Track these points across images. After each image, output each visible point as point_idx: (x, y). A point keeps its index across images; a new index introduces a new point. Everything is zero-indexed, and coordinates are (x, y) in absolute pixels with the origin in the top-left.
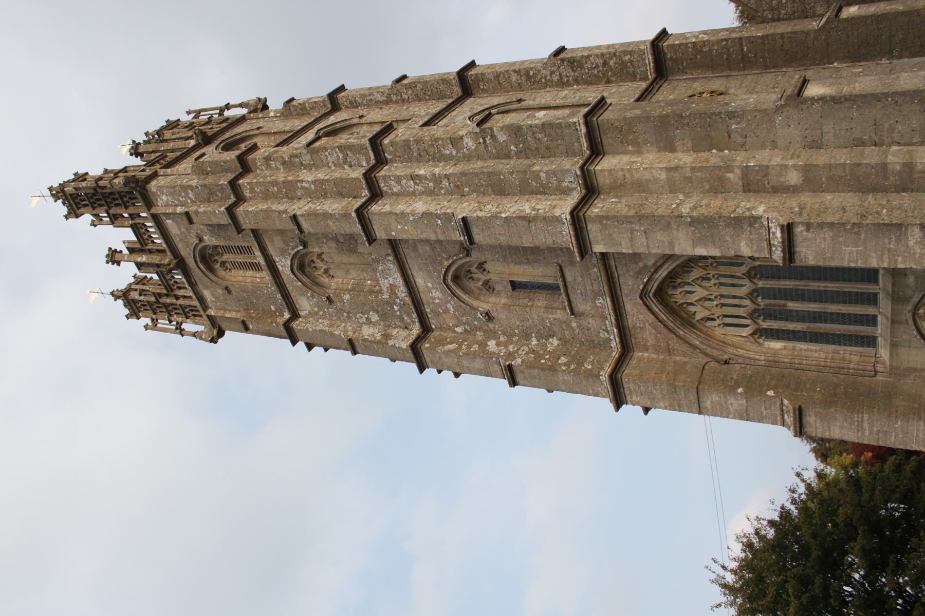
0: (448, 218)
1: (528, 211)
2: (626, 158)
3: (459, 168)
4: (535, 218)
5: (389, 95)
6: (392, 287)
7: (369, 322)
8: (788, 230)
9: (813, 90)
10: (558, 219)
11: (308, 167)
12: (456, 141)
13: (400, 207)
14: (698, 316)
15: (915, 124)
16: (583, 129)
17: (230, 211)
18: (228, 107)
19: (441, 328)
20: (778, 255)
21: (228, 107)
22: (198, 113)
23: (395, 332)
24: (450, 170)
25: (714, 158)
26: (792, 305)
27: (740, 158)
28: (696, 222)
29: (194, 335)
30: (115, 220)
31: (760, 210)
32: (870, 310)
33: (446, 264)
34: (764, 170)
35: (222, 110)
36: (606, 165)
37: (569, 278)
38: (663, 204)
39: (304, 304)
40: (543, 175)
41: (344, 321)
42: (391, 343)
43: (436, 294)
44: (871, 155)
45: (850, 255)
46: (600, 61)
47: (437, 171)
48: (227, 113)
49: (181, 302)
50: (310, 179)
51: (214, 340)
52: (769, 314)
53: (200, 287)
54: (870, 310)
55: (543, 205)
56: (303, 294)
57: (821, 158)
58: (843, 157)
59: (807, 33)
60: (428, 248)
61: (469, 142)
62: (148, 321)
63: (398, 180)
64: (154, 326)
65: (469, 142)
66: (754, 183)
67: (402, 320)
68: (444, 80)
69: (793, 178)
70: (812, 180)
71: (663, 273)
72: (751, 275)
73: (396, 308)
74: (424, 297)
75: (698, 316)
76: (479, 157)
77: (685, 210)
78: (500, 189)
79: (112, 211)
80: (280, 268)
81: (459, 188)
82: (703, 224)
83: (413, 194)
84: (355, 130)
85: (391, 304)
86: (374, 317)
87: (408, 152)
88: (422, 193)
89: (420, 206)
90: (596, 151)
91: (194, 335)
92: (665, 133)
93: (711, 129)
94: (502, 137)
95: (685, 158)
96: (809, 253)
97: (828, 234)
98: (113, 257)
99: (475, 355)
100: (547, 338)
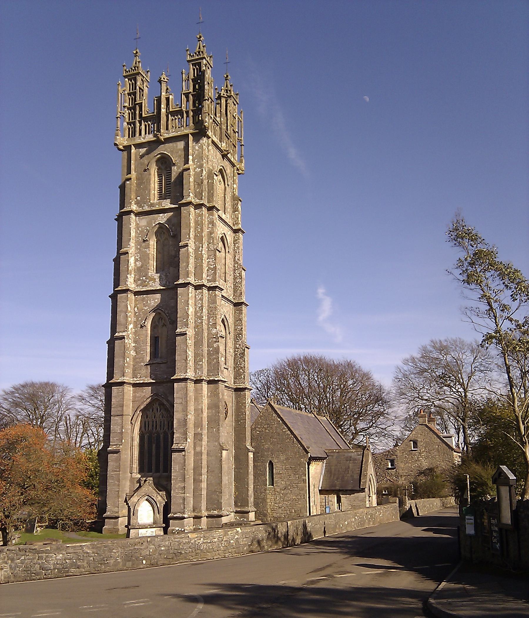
0: (187, 325)
1: (189, 359)
2: (206, 393)
3: (205, 327)
4: (187, 363)
5: (237, 263)
7: (136, 260)
8: (183, 450)
9: (224, 452)
10: (186, 372)
11: (208, 247)
12: (215, 325)
13: (190, 302)
14: (148, 413)
15: (213, 482)
16: (216, 379)
17: (190, 203)
19: (136, 300)
23: (133, 275)
24: (205, 322)
25: (205, 423)
26: (154, 446)
27: (205, 432)
28: (185, 420)
31: (189, 440)
32: (153, 470)
33: (166, 312)
34: (201, 440)
36: (205, 385)
37: (162, 365)
38: (191, 408)
39: (144, 221)
40: (201, 363)
41: (136, 245)
42: (129, 276)
44: (204, 471)
45: (175, 468)
46: (242, 366)
47: (204, 318)
49: (138, 124)
50: (203, 252)
52: (150, 438)
54: (153, 470)
55: (191, 363)
56: (149, 224)
57: (204, 457)
58: (204, 463)
59: (245, 442)
60: (172, 305)
61: (214, 331)
63: (201, 299)
65: (214, 331)
66: (198, 437)
67: (139, 280)
69: (198, 449)
70: (198, 455)
71: (165, 403)
72: (166, 434)
73: (144, 278)
75: (148, 413)
76: (208, 334)
77: (189, 417)
78: (198, 343)
79: (191, 97)
80: (161, 215)
81: (198, 327)
82: (185, 422)
83: (195, 305)
84: (223, 249)
86: (139, 264)
87: (213, 301)
88: (196, 309)
89: (191, 310)
90: (210, 382)
92: (214, 406)
93: (214, 422)
94: (215, 345)
95: (205, 414)
96: (174, 455)
97: (182, 461)
99: (127, 320)
100: (135, 350)
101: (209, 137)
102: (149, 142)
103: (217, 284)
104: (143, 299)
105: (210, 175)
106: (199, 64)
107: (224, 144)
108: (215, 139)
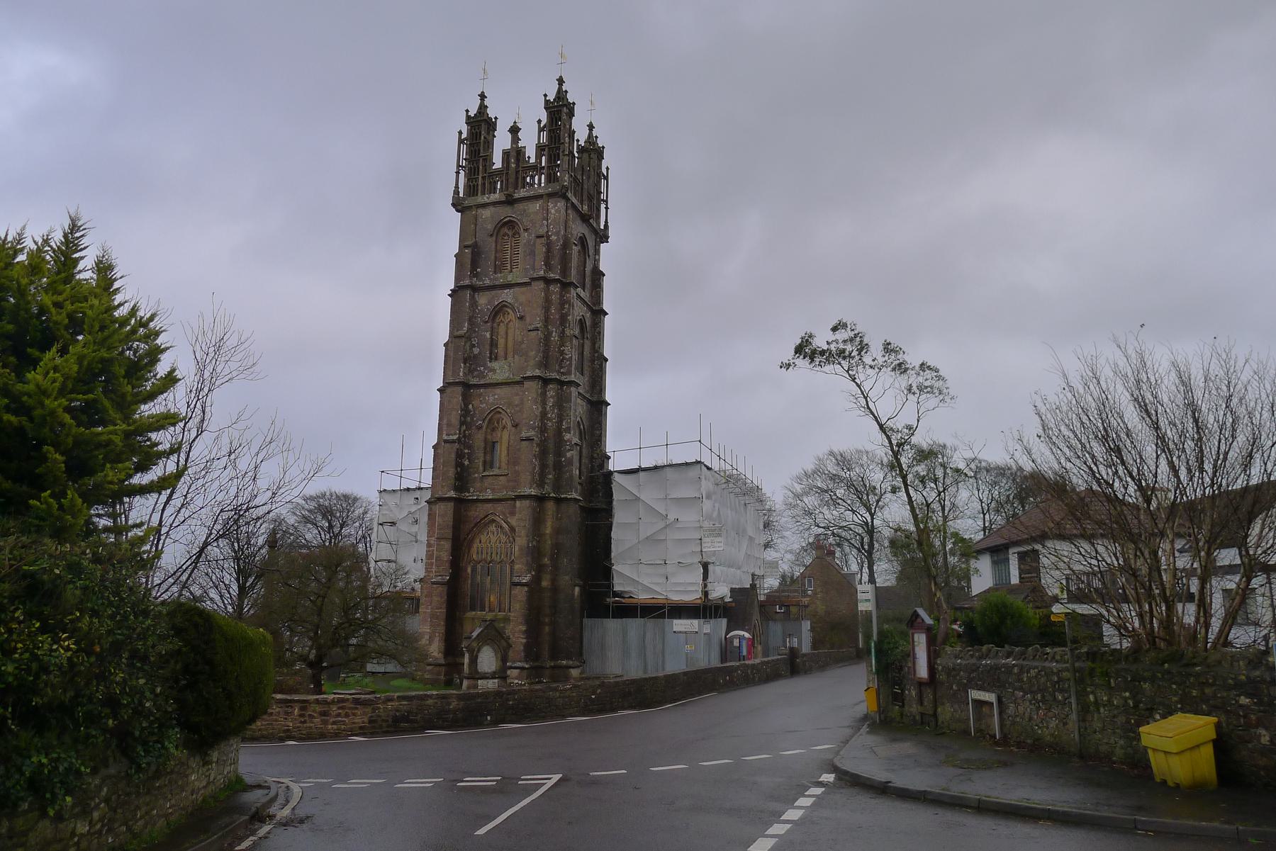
6: (494, 370)
18: (607, 208)
20: (516, 580)
21: (607, 208)
22: (606, 178)
29: (457, 187)
30: (540, 149)
35: (606, 201)
43: (491, 399)
48: (603, 206)
51: (453, 205)
53: (492, 208)
56: (489, 303)
62: (464, 136)
64: (461, 141)
68: (601, 390)
71: (505, 525)
74: (489, 390)
85: (485, 365)
91: (457, 187)
98: (514, 130)
101: (568, 199)
102: (494, 204)
103: (572, 378)
104: (480, 395)
105: (566, 245)
106: (559, 112)
107: (585, 207)
108: (575, 201)
